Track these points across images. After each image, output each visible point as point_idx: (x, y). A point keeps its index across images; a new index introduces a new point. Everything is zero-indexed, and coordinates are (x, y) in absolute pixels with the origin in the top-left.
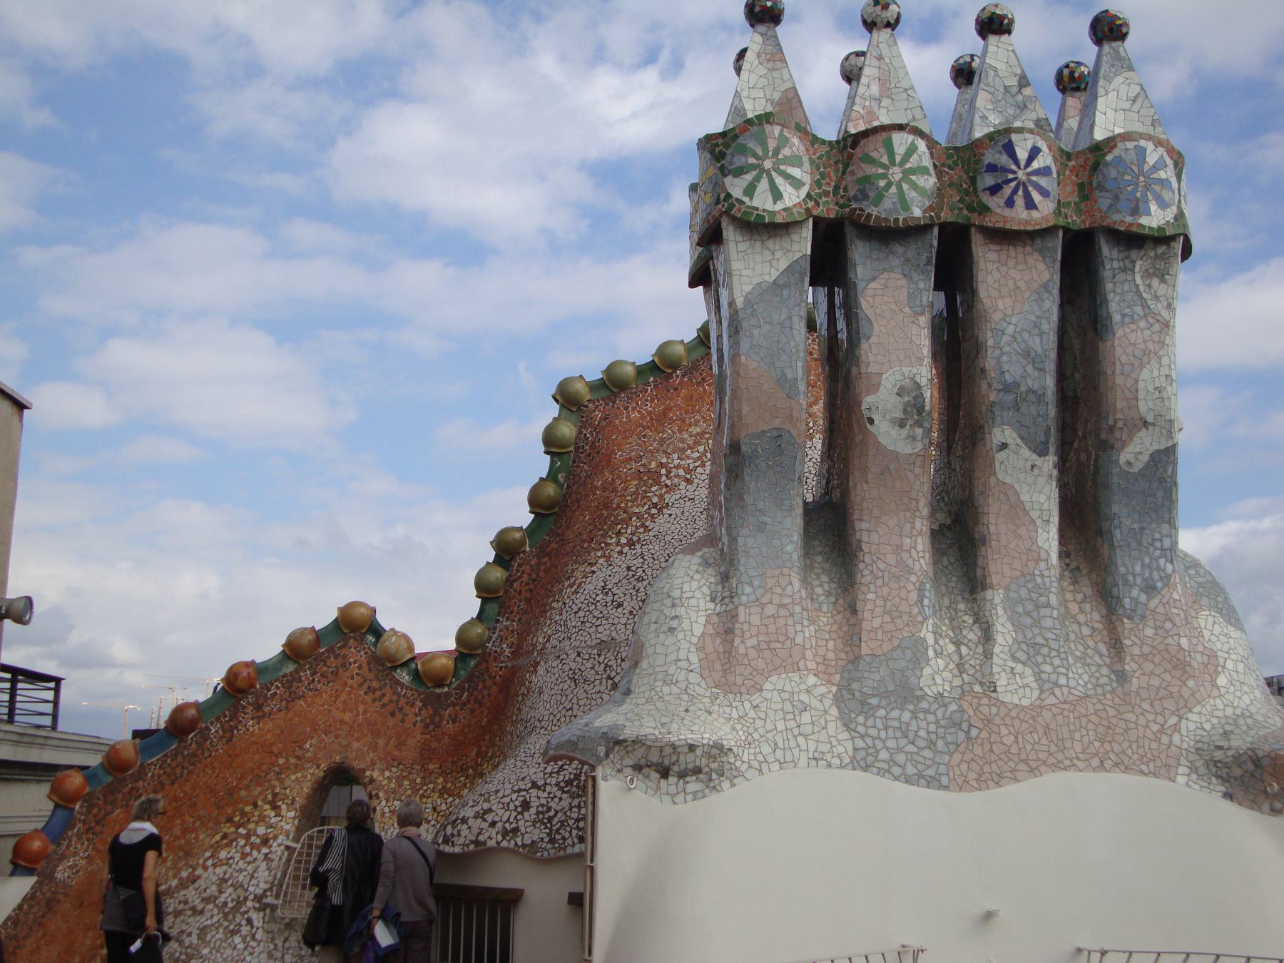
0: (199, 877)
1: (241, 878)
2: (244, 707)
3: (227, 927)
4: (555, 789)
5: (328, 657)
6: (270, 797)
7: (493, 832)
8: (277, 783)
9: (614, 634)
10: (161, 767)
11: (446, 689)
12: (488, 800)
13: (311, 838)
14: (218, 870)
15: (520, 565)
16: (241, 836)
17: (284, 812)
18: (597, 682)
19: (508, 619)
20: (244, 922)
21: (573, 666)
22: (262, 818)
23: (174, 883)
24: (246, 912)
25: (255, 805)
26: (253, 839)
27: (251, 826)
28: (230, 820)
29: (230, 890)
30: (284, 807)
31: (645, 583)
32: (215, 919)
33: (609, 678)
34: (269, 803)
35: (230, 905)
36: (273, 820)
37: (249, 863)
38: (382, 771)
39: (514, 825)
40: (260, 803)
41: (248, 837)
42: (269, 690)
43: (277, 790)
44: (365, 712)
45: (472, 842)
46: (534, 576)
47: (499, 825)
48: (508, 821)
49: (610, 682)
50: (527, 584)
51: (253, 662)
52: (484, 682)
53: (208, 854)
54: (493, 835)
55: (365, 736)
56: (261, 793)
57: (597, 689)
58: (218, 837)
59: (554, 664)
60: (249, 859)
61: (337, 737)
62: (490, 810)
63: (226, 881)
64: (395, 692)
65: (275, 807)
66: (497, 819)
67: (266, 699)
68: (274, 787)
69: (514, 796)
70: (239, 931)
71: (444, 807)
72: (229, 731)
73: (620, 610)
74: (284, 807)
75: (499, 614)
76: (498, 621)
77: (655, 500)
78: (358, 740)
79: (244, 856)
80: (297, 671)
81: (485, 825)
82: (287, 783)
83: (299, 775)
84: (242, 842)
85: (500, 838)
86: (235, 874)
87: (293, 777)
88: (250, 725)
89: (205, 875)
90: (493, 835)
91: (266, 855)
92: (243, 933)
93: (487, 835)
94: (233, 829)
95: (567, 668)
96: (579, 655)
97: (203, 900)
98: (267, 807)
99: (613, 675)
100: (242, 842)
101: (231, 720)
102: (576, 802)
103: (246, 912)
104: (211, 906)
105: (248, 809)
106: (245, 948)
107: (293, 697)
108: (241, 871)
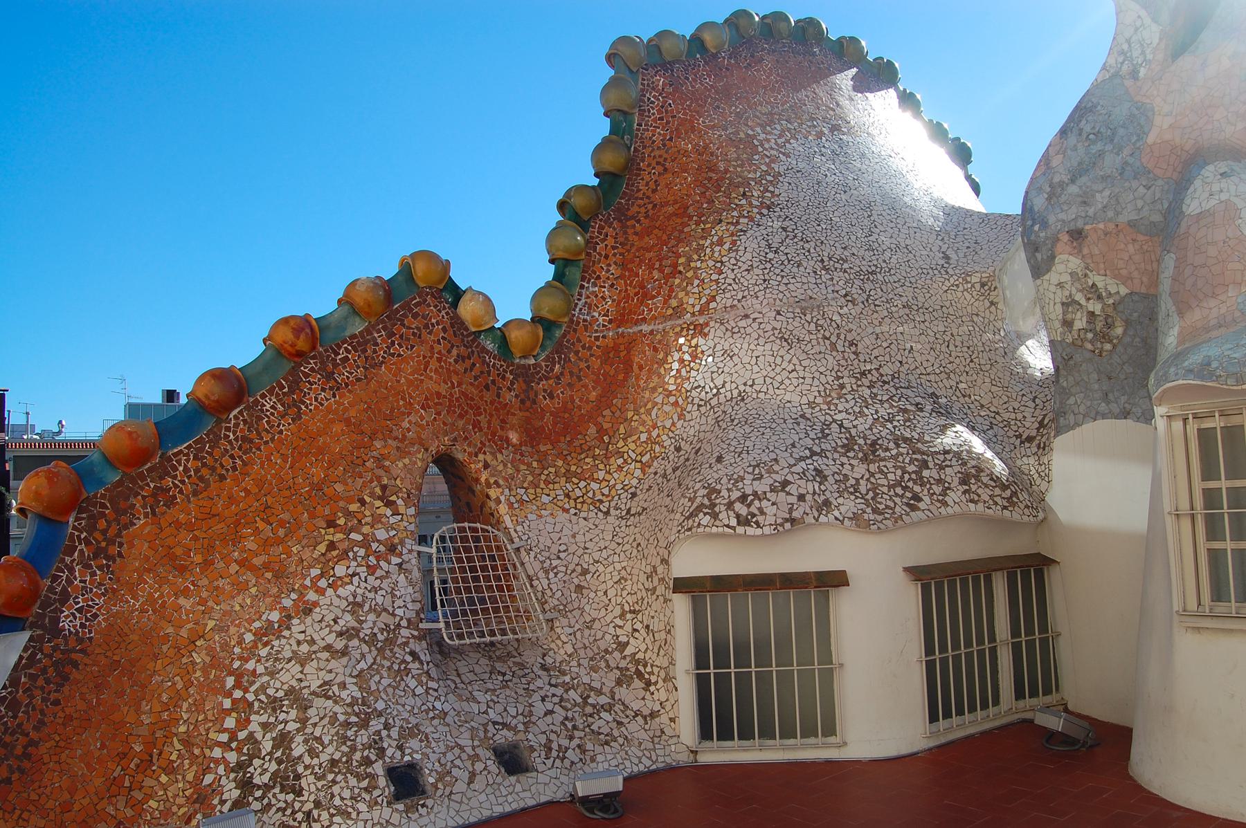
0: (316, 604)
1: (380, 600)
2: (307, 376)
3: (389, 668)
4: (836, 456)
5: (405, 316)
6: (378, 491)
7: (804, 507)
8: (381, 472)
9: (809, 292)
10: (196, 458)
11: (532, 361)
12: (770, 471)
13: (443, 539)
14: (341, 591)
15: (601, 228)
16: (357, 543)
17: (402, 510)
18: (814, 342)
19: (595, 285)
20: (409, 658)
21: (778, 325)
22: (377, 519)
23: (275, 616)
24: (406, 644)
25: (363, 502)
26: (374, 546)
27: (366, 529)
28: (331, 524)
29: (372, 617)
30: (400, 502)
31: (812, 244)
32: (370, 660)
33: (825, 338)
34: (381, 498)
35: (380, 637)
36: (392, 520)
37: (381, 578)
38: (493, 454)
39: (823, 498)
40: (368, 499)
41: (365, 544)
42: (337, 354)
43: (385, 482)
44: (460, 384)
45: (786, 520)
46: (622, 240)
47: (809, 497)
48: (814, 493)
49: (827, 342)
50: (614, 248)
51: (306, 319)
52: (577, 353)
53: (315, 572)
54: (808, 510)
55: (467, 412)
56: (364, 485)
57: (817, 349)
58: (322, 548)
59: (743, 323)
60: (379, 573)
61: (438, 414)
62: (785, 483)
63: (361, 606)
64: (484, 362)
65: (389, 504)
66: (803, 491)
67: (335, 365)
68: (379, 479)
69: (803, 464)
70: (408, 671)
71: (578, 493)
72: (293, 408)
73: (802, 269)
74: (400, 502)
75: (583, 279)
76: (582, 287)
77: (764, 168)
78: (461, 416)
79: (372, 570)
80: (368, 330)
81: (793, 500)
82: (395, 472)
83: (407, 461)
84: (362, 552)
85: (816, 514)
86: (371, 595)
87: (400, 465)
88: (316, 396)
89: (323, 601)
90: (808, 510)
91: (400, 565)
92: (414, 672)
93: (801, 510)
94: (341, 536)
95: (769, 327)
96: (778, 313)
97: (340, 634)
98: (378, 503)
99: (827, 334)
100: (362, 552)
101: (291, 391)
102: (873, 468)
103: (406, 644)
104: (355, 642)
105: (354, 507)
106: (427, 692)
107: (372, 364)
108: (375, 590)
